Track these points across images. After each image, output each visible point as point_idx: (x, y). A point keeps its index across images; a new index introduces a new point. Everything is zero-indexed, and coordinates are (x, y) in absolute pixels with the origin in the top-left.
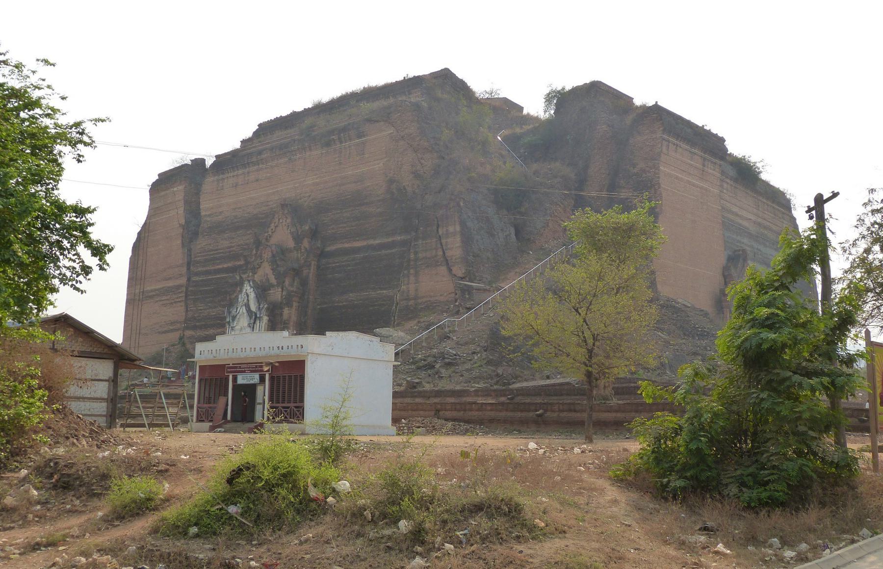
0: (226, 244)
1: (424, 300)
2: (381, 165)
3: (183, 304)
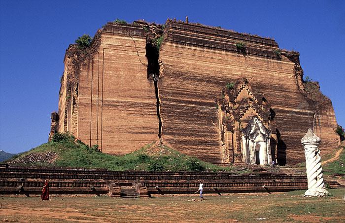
2: (291, 76)
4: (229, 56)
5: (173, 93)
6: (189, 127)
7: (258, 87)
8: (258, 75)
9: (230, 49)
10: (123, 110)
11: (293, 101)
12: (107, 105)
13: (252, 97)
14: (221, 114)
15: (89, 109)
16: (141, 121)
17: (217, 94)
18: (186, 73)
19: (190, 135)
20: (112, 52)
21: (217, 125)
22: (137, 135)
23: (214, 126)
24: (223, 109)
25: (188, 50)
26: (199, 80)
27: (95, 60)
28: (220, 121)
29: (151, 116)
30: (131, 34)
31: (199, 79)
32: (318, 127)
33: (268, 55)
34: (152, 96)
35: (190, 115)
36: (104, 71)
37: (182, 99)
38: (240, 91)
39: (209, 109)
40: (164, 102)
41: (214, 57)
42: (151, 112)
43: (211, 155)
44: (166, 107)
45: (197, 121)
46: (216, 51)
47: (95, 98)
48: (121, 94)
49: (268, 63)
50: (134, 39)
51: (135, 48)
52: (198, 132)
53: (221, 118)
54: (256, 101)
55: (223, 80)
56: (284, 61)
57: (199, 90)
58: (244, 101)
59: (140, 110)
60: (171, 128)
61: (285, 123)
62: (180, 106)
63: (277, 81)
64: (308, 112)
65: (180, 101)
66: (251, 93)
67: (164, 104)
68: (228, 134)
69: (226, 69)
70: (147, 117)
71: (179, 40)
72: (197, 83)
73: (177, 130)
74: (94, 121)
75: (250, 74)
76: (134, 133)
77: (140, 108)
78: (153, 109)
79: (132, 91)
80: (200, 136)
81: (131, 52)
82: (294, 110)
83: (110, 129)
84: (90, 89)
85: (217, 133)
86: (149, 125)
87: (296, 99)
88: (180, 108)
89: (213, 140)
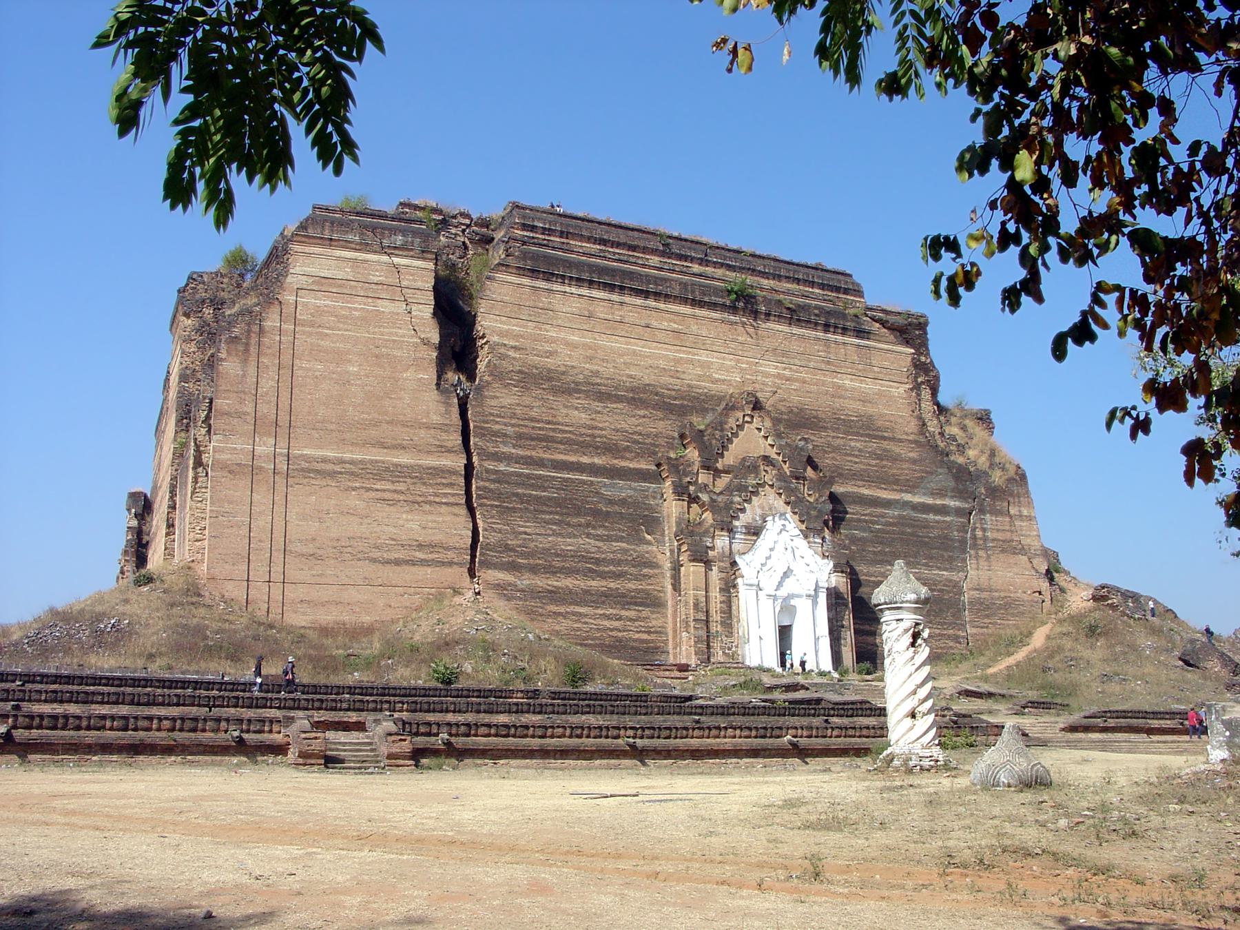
0: (583, 417)
1: (1002, 594)
2: (901, 390)
3: (463, 511)
4: (706, 324)
5: (520, 436)
6: (569, 544)
7: (794, 421)
8: (795, 386)
9: (706, 299)
10: (354, 489)
11: (905, 471)
12: (303, 470)
13: (772, 453)
14: (672, 508)
15: (245, 482)
16: (411, 524)
17: (661, 441)
18: (564, 373)
19: (570, 572)
20: (323, 302)
21: (657, 541)
22: (399, 569)
23: (649, 543)
24: (681, 491)
25: (569, 300)
26: (603, 397)
27: (268, 324)
28: (670, 528)
29: (444, 509)
30: (386, 242)
31: (603, 394)
32: (981, 553)
33: (832, 322)
34: (449, 444)
35: (572, 508)
36: (297, 362)
37: (547, 456)
38: (735, 435)
39: (635, 489)
40: (491, 465)
41: (654, 324)
42: (445, 495)
43: (637, 636)
44: (494, 481)
45: (594, 528)
46: (662, 306)
47: (265, 447)
48: (348, 436)
49: (829, 347)
50: (396, 260)
51: (400, 292)
52: (598, 562)
53: (673, 520)
54: (786, 467)
55: (683, 398)
56: (879, 341)
57: (601, 429)
58: (748, 467)
59: (412, 487)
60: (508, 548)
61: (878, 538)
62: (539, 477)
63: (857, 406)
64: (952, 503)
65: (540, 463)
66: (770, 441)
67: (487, 471)
68: (692, 572)
69: (691, 361)
70: (430, 513)
71: (543, 269)
72: (597, 405)
73: (531, 554)
74: (262, 523)
75: (769, 381)
76: (388, 562)
77: (409, 480)
78: (451, 485)
79: (385, 426)
80: (603, 575)
81: (386, 303)
82: (907, 497)
83: (310, 549)
84: (250, 419)
85: (653, 565)
86: (438, 537)
87: (914, 462)
88: (541, 484)
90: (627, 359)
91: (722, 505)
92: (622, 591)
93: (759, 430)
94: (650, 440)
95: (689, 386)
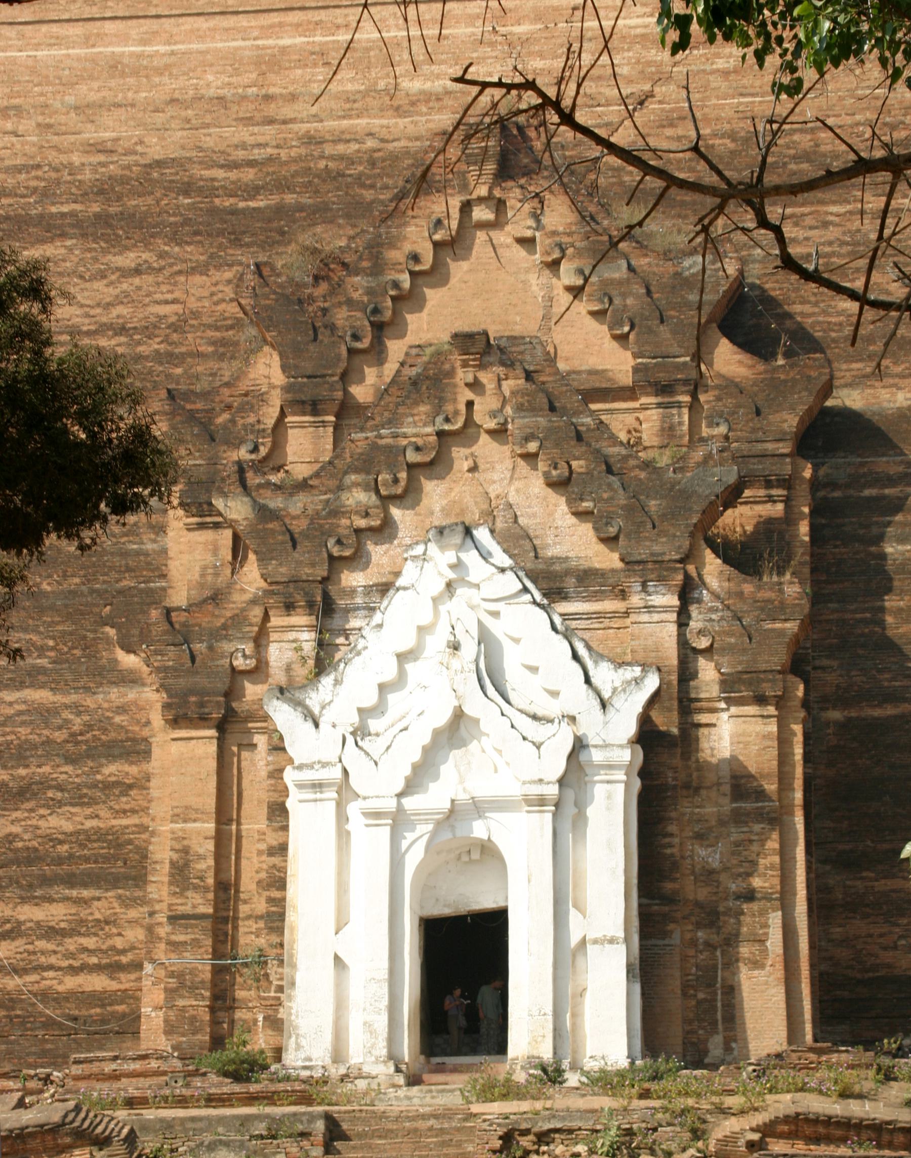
17: (194, 340)
23: (130, 679)
38: (436, 274)
43: (71, 983)
55: (282, 185)
89: (100, 835)
90: (88, 92)
91: (300, 526)
92: (27, 840)
93: (527, 243)
94: (155, 345)
95: (310, 140)
